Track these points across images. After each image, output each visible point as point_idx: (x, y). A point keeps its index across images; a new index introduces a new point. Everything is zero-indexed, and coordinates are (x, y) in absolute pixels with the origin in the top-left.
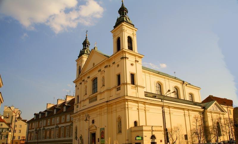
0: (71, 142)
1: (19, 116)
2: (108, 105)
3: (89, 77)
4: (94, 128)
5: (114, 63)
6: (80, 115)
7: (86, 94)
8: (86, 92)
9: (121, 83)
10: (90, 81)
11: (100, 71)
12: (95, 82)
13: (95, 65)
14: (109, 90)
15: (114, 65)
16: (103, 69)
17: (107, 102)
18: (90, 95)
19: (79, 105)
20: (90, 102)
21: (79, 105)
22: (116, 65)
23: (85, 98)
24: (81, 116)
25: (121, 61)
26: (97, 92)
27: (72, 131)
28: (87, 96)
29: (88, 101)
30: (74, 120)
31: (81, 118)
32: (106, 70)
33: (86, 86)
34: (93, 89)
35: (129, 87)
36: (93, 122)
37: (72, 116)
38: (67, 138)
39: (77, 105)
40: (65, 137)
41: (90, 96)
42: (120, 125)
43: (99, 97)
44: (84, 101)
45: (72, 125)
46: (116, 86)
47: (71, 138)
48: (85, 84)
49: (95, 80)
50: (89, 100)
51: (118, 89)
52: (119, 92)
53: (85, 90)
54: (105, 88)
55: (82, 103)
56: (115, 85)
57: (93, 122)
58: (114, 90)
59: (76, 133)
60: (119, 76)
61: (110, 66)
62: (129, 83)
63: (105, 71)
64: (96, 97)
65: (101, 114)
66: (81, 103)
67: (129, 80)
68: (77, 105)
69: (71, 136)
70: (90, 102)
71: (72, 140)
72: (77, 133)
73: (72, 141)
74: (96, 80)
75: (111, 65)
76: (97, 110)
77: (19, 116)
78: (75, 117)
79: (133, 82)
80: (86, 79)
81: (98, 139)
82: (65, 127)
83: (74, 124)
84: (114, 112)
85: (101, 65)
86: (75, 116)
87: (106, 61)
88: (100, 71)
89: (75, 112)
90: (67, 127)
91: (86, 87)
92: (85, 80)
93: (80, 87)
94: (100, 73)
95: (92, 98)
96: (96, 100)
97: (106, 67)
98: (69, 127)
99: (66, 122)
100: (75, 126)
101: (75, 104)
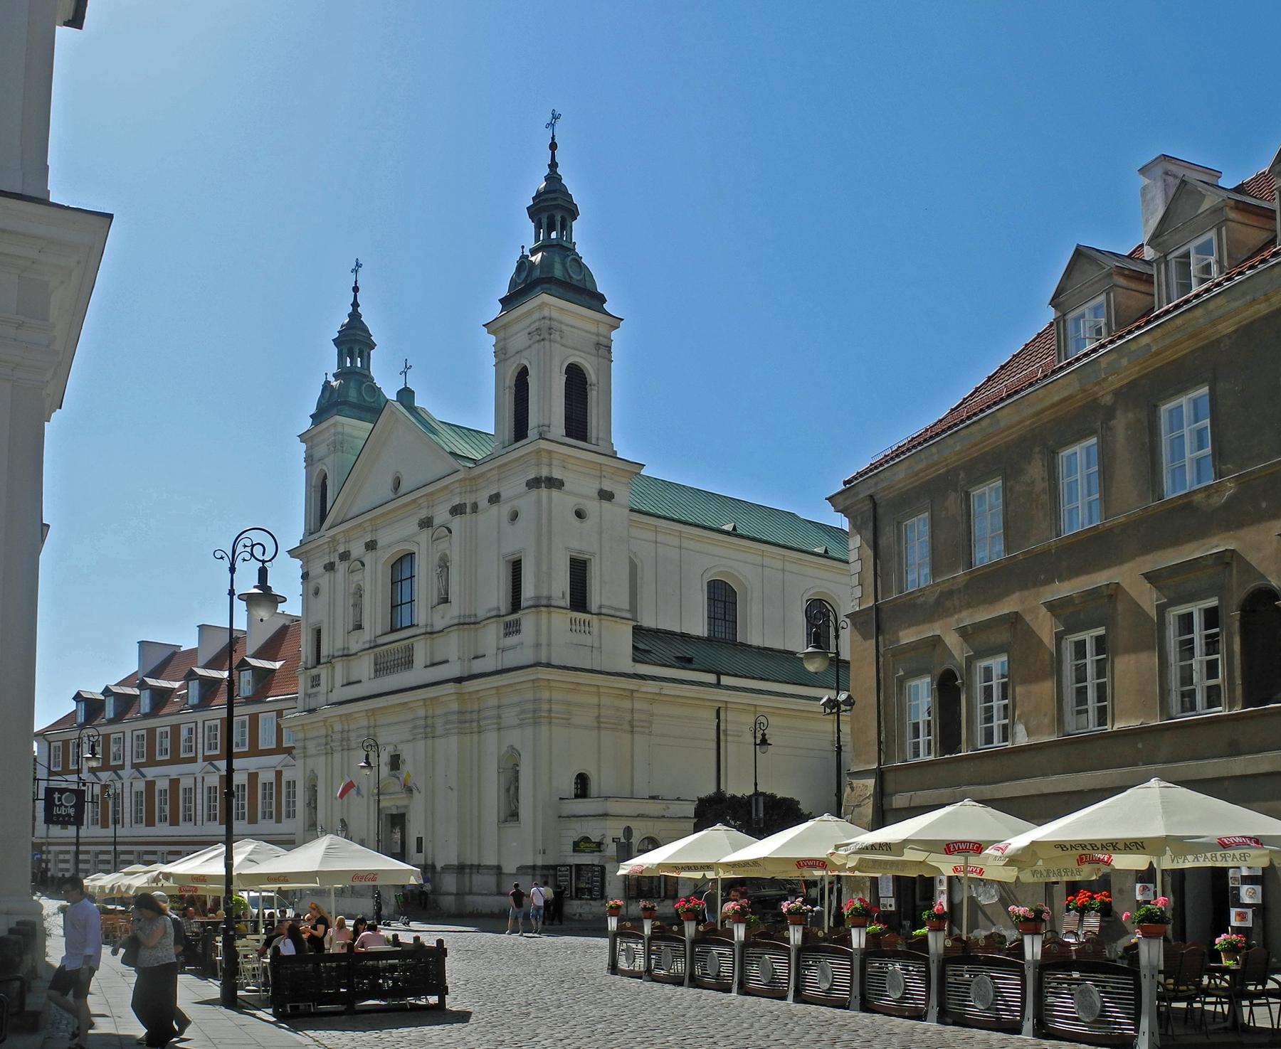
1: (263, 573)
3: (371, 546)
7: (359, 627)
10: (380, 567)
11: (426, 523)
12: (406, 574)
13: (402, 490)
14: (468, 623)
15: (495, 508)
16: (441, 515)
17: (459, 680)
20: (381, 668)
21: (323, 672)
22: (505, 509)
26: (412, 626)
28: (366, 636)
32: (457, 523)
34: (392, 607)
35: (561, 620)
36: (395, 762)
41: (380, 641)
42: (512, 789)
49: (402, 566)
51: (512, 629)
53: (355, 605)
54: (454, 611)
55: (339, 666)
57: (395, 762)
61: (475, 508)
64: (410, 649)
67: (561, 586)
72: (315, 808)
74: (406, 565)
75: (483, 503)
77: (263, 573)
79: (579, 600)
84: (487, 727)
87: (460, 481)
91: (359, 593)
92: (437, 521)
94: (426, 533)
96: (408, 663)
97: (457, 510)
100: (308, 773)
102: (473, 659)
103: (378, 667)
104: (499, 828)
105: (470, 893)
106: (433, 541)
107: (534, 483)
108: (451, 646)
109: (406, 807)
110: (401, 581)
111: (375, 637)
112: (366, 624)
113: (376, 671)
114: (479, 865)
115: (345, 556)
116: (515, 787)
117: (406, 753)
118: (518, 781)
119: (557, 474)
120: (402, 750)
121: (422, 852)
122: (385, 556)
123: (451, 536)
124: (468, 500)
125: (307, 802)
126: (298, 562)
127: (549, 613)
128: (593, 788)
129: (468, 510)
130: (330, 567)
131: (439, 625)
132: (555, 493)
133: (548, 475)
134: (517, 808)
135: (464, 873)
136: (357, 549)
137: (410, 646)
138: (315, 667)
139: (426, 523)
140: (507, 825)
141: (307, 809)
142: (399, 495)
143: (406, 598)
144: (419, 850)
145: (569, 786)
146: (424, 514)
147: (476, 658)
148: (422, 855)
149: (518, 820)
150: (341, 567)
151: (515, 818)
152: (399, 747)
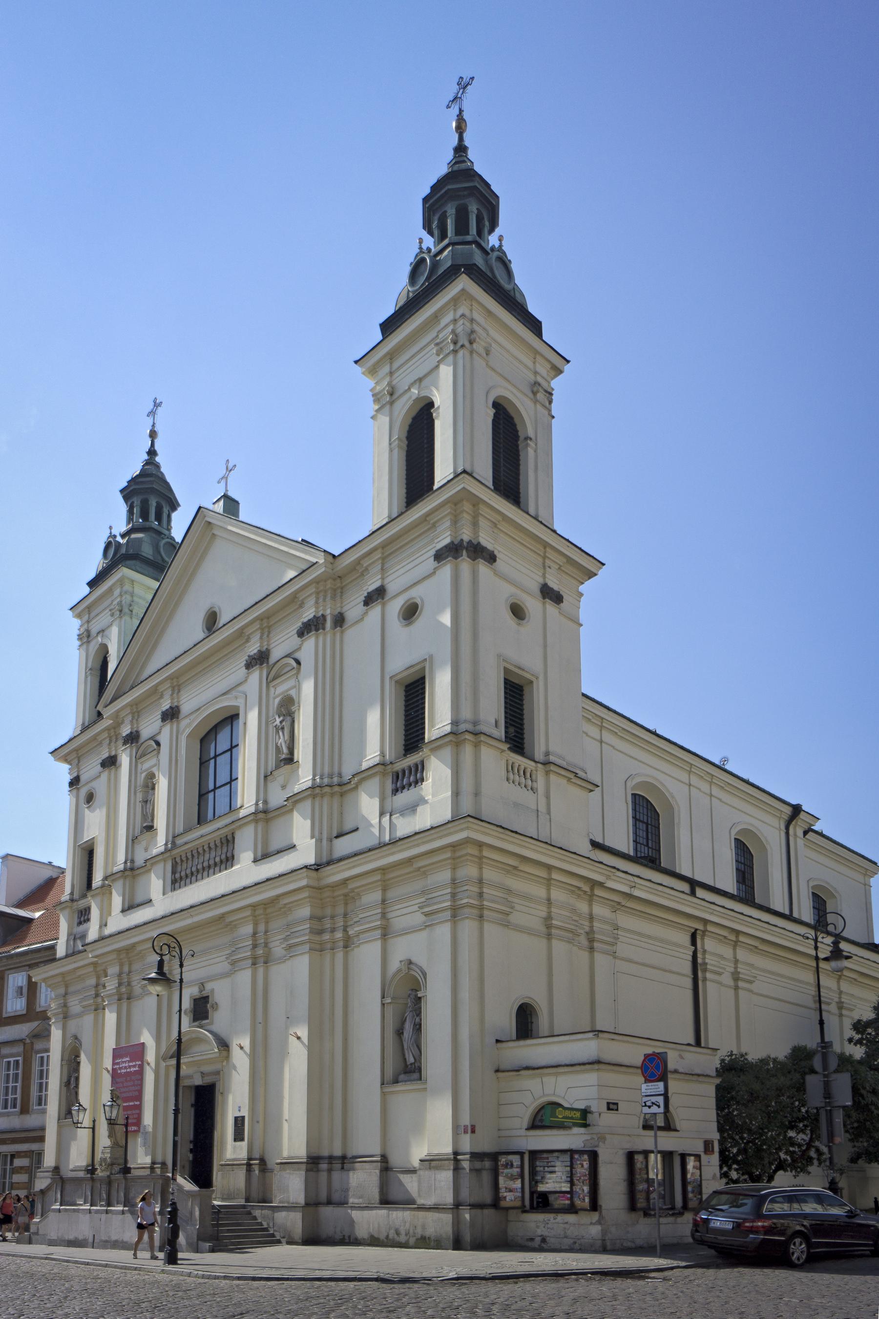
0: (34, 1147)
2: (319, 888)
5: (377, 596)
9: (430, 734)
15: (375, 611)
20: (177, 881)
25: (436, 569)
27: (43, 1074)
37: (44, 980)
47: (31, 1121)
63: (298, 662)
66: (106, 888)
68: (82, 904)
71: (43, 1129)
73: (41, 1139)
81: (239, 1122)
88: (261, 659)
93: (100, 787)
95: (195, 854)
98: (19, 1049)
102: (337, 837)
103: (177, 876)
104: (383, 1094)
105: (329, 1203)
106: (268, 684)
109: (218, 1073)
110: (216, 757)
111: (174, 837)
113: (174, 882)
114: (343, 1158)
115: (133, 738)
116: (415, 1025)
117: (220, 992)
118: (419, 1014)
119: (486, 540)
120: (213, 990)
121: (242, 1140)
122: (188, 725)
123: (299, 670)
127: (477, 745)
132: (483, 568)
134: (418, 1058)
135: (318, 1171)
136: (150, 725)
137: (229, 837)
140: (399, 1087)
141: (64, 1089)
143: (223, 778)
144: (239, 1136)
145: (508, 1022)
148: (244, 1144)
149: (420, 1079)
151: (416, 1075)
152: (209, 986)
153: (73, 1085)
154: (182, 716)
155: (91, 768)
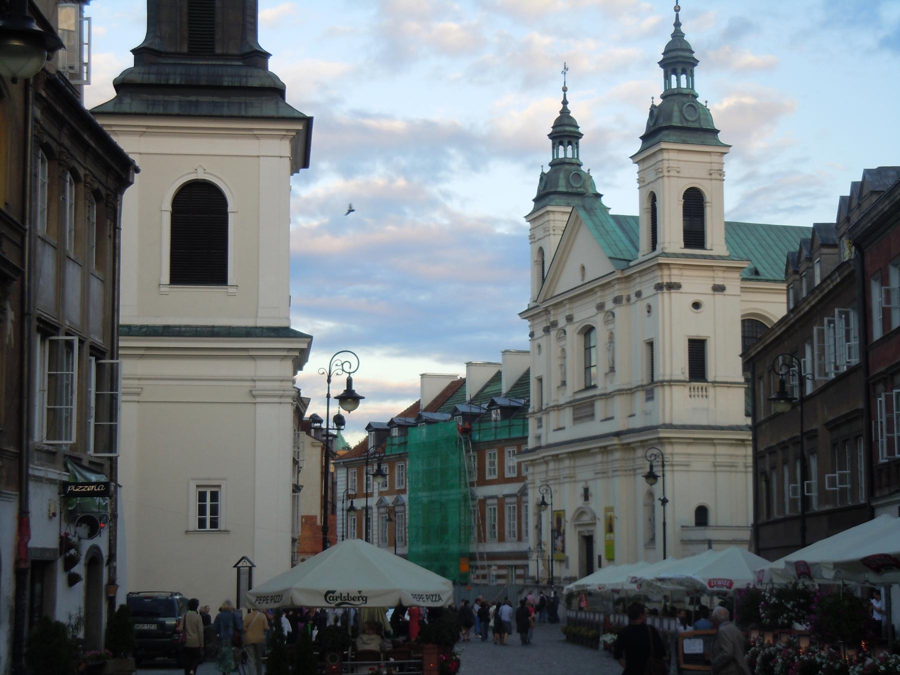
4: (586, 519)
6: (547, 463)
7: (564, 383)
8: (564, 374)
17: (618, 434)
18: (576, 390)
19: (544, 418)
20: (577, 419)
23: (562, 401)
24: (552, 465)
29: (568, 413)
30: (530, 478)
31: (551, 474)
33: (563, 350)
38: (508, 547)
39: (538, 415)
40: (502, 539)
43: (599, 407)
44: (558, 408)
45: (523, 492)
46: (645, 383)
48: (559, 339)
50: (574, 410)
51: (650, 397)
52: (650, 403)
56: (642, 380)
58: (640, 396)
59: (537, 527)
60: (651, 344)
61: (628, 299)
62: (682, 378)
64: (592, 405)
65: (603, 474)
69: (524, 537)
70: (577, 419)
75: (633, 298)
76: (594, 454)
78: (533, 465)
80: (562, 323)
82: (501, 501)
83: (530, 492)
85: (604, 287)
86: (533, 463)
87: (618, 279)
89: (531, 443)
90: (508, 500)
97: (617, 300)
98: (514, 500)
99: (502, 480)
101: (530, 410)
107: (659, 287)
108: (619, 406)
112: (568, 383)
124: (624, 294)
125: (536, 524)
126: (527, 323)
128: (712, 519)
129: (624, 301)
130: (547, 330)
131: (610, 388)
133: (668, 281)
138: (539, 412)
139: (601, 307)
142: (586, 281)
146: (599, 301)
147: (630, 416)
150: (553, 333)
153: (539, 527)
154: (575, 320)
155: (539, 333)
